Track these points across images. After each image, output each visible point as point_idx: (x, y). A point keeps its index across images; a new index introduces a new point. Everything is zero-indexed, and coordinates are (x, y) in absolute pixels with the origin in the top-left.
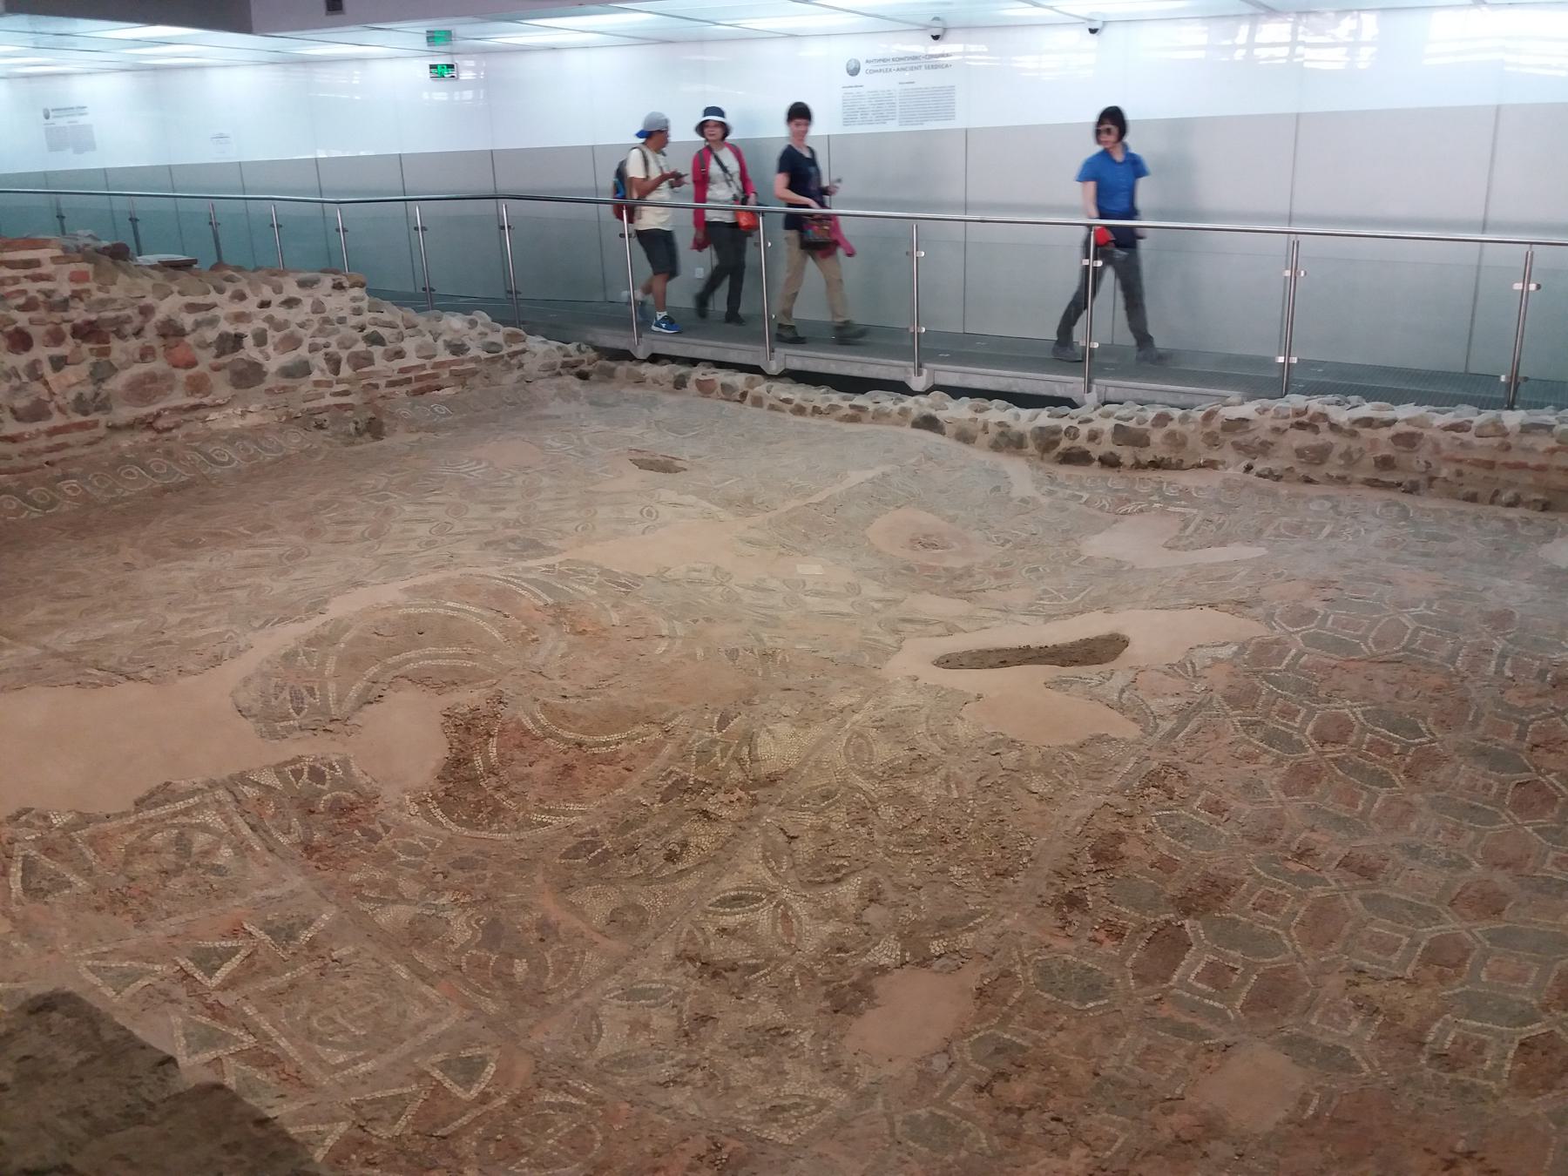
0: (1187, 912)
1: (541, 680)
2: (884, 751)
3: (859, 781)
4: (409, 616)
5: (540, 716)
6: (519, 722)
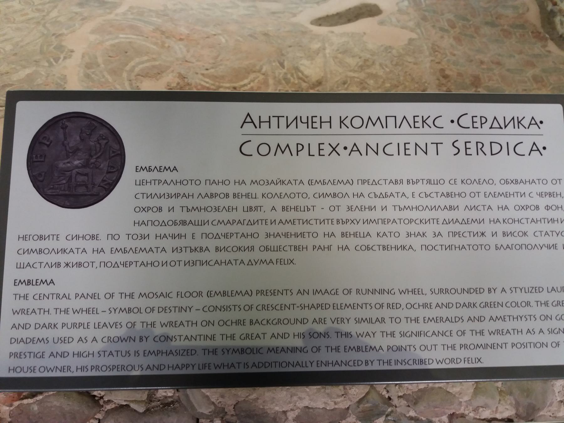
0: (476, 87)
1: (190, 64)
2: (352, 62)
3: (352, 74)
4: (113, 45)
5: (207, 80)
6: (200, 84)
